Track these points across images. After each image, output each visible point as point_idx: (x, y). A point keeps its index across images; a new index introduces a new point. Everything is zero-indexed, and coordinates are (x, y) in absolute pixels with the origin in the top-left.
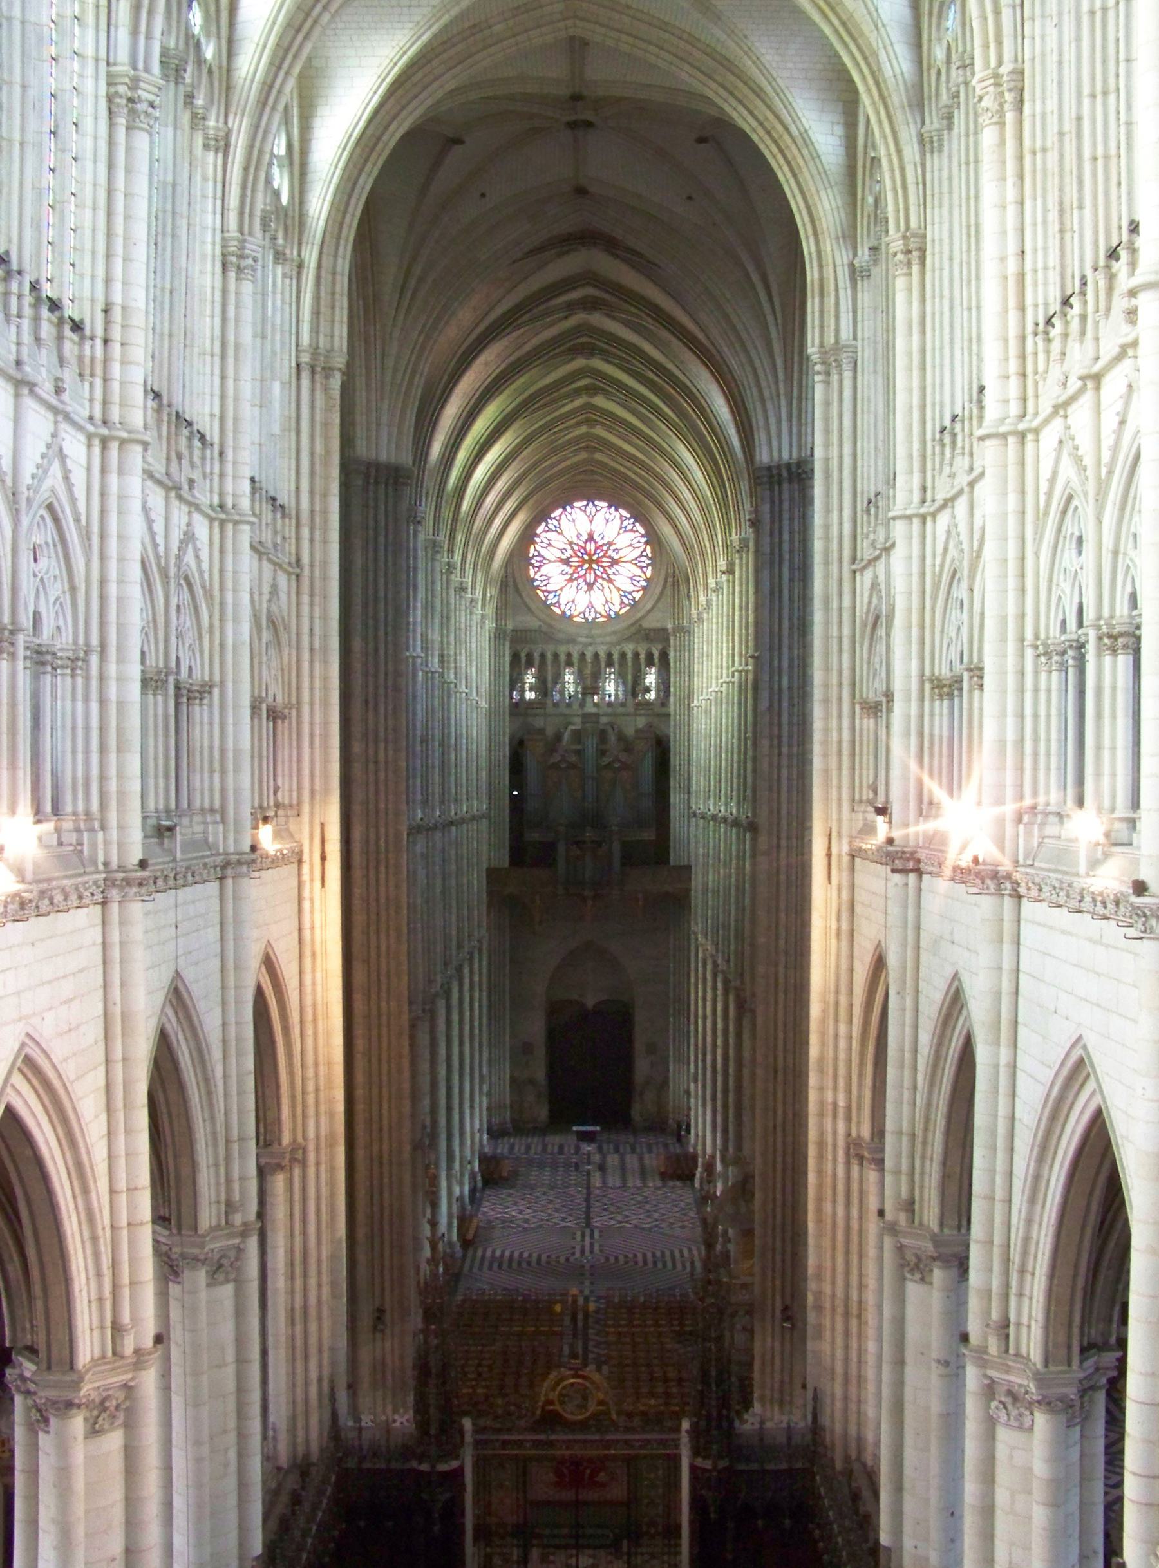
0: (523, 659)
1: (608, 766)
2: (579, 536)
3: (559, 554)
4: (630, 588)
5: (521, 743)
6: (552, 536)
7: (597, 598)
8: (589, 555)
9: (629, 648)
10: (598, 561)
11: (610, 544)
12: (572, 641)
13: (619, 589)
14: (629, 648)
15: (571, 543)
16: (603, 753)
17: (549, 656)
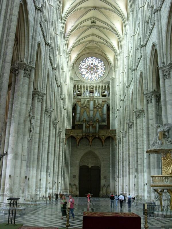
0: (77, 87)
1: (95, 108)
2: (89, 64)
3: (85, 67)
4: (100, 74)
5: (75, 105)
6: (84, 64)
7: (93, 76)
8: (92, 68)
9: (101, 85)
10: (94, 69)
11: (96, 65)
12: (88, 83)
13: (98, 75)
14: (101, 85)
15: (88, 65)
16: (94, 105)
17: (82, 86)
